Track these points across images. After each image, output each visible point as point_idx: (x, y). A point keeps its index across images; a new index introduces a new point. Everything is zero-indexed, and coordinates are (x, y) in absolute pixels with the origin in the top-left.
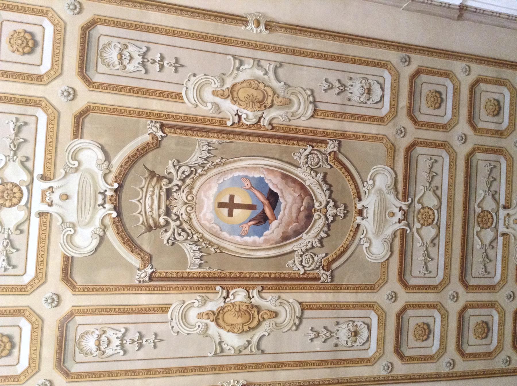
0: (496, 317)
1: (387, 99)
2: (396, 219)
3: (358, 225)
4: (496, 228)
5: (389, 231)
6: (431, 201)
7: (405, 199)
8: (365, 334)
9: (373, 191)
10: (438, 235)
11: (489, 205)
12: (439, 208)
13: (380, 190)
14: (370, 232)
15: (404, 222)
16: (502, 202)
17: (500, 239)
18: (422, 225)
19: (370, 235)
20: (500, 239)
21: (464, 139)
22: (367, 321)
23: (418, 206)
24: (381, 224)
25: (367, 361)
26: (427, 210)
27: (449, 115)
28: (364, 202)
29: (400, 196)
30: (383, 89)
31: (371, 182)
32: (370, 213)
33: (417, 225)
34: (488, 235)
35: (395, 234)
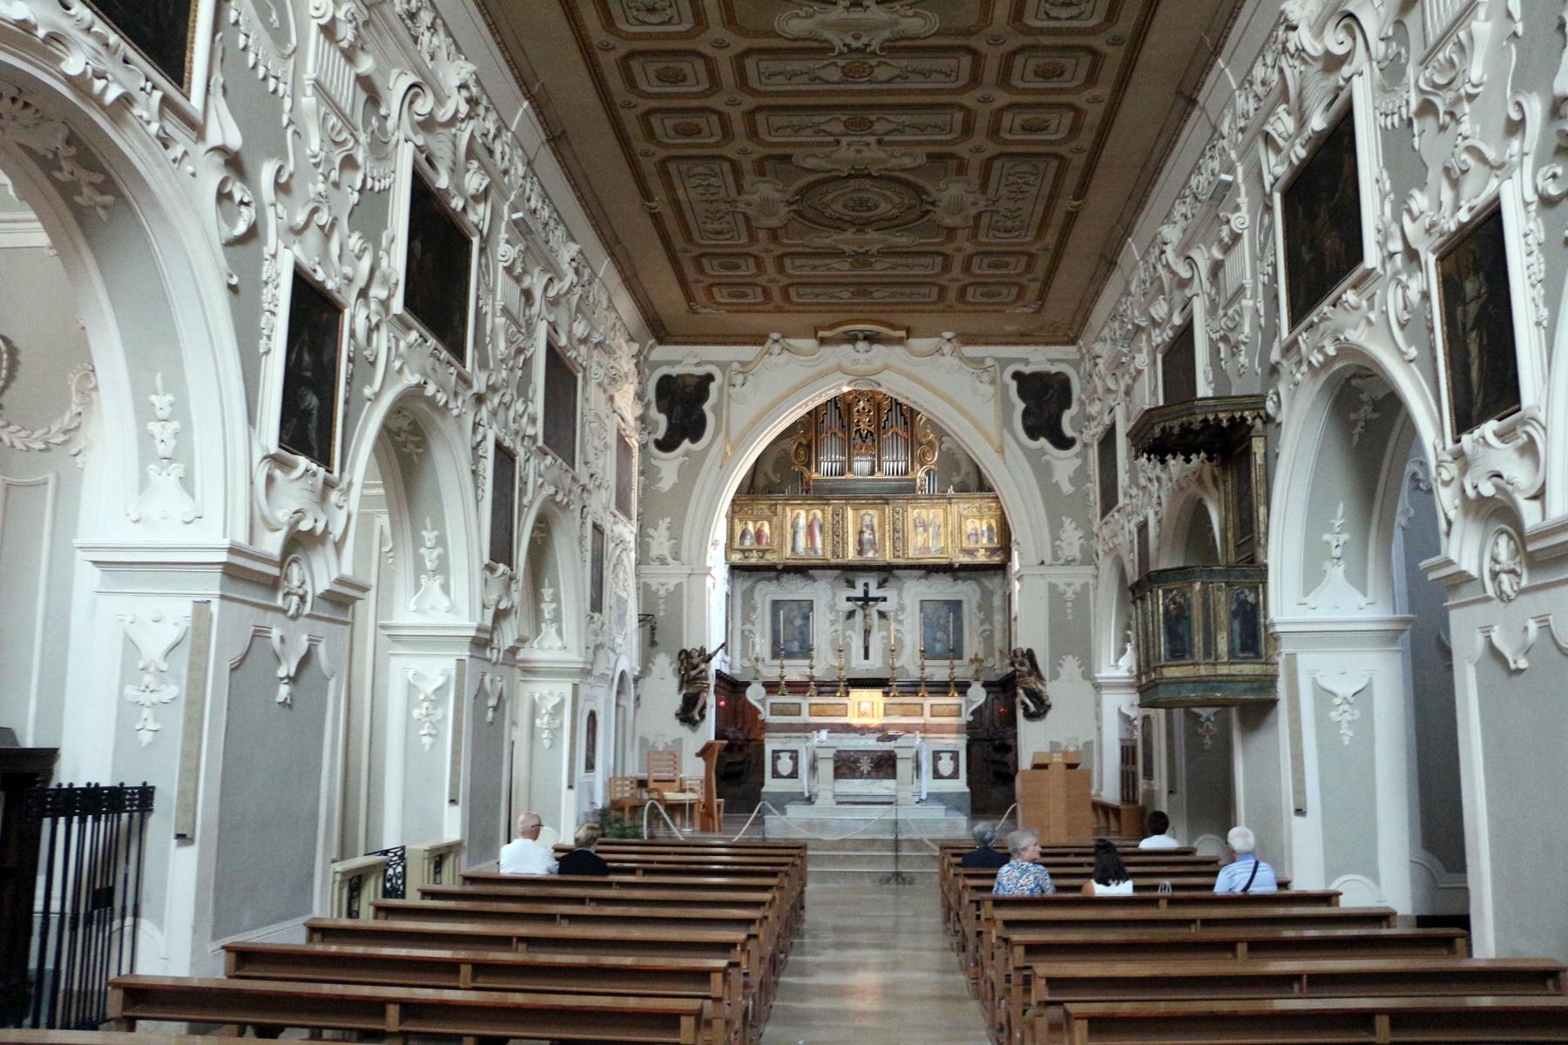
0: (712, 140)
1: (1052, 24)
2: (849, 40)
3: (835, 3)
4: (844, 135)
5: (828, 34)
6: (881, 73)
7: (882, 49)
8: (655, 19)
9: (894, 16)
10: (827, 82)
11: (879, 127)
12: (870, 82)
13: (897, 23)
14: (823, 16)
15: (846, 50)
16: (887, 138)
17: (831, 139)
18: (843, 68)
19: (818, 17)
20: (831, 139)
21: (986, 100)
22: (676, 20)
23: (873, 62)
24: (840, 26)
25: (608, 22)
26: (868, 71)
27: (1021, 85)
28: (874, 7)
29: (888, 44)
30: (1071, 18)
31: (910, 13)
32: (857, 14)
33: (842, 63)
34: (838, 128)
35: (825, 41)
